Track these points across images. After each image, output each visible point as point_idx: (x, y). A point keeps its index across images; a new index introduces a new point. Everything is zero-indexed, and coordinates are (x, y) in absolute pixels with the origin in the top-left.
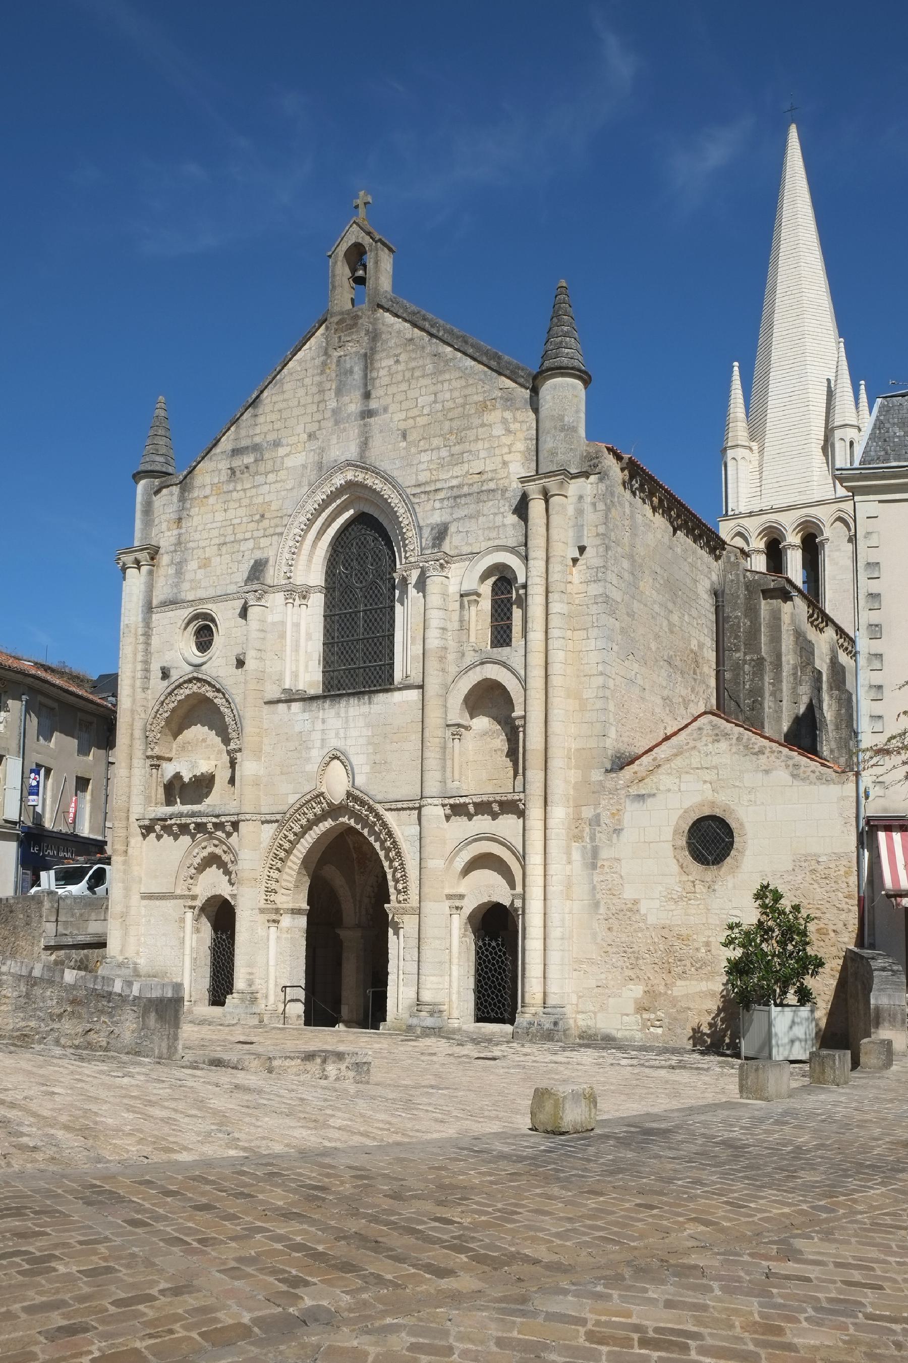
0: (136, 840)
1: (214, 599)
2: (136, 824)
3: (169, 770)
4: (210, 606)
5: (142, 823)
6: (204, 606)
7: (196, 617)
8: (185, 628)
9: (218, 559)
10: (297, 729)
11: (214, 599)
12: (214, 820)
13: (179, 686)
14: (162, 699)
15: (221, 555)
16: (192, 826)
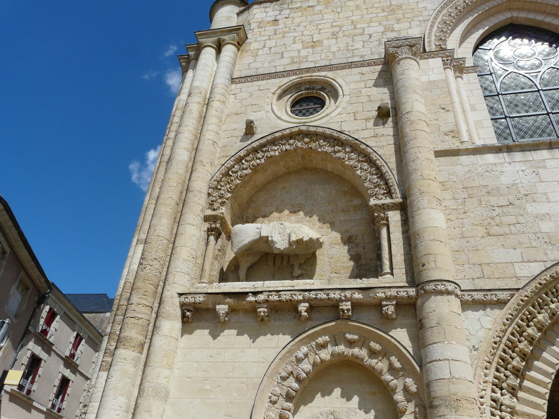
0: (171, 325)
1: (330, 67)
2: (177, 301)
3: (247, 232)
4: (323, 73)
5: (190, 299)
6: (314, 74)
7: (296, 86)
8: (280, 97)
9: (333, 41)
10: (505, 180)
11: (330, 67)
12: (358, 296)
13: (273, 142)
14: (242, 154)
15: (337, 38)
16: (303, 307)
